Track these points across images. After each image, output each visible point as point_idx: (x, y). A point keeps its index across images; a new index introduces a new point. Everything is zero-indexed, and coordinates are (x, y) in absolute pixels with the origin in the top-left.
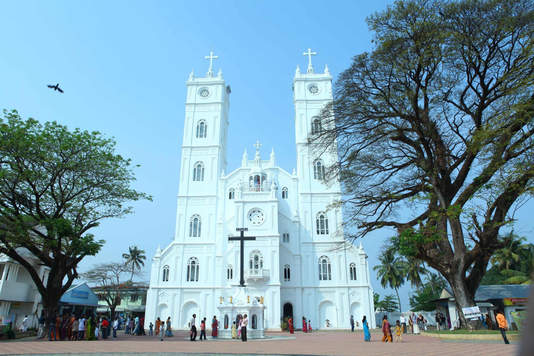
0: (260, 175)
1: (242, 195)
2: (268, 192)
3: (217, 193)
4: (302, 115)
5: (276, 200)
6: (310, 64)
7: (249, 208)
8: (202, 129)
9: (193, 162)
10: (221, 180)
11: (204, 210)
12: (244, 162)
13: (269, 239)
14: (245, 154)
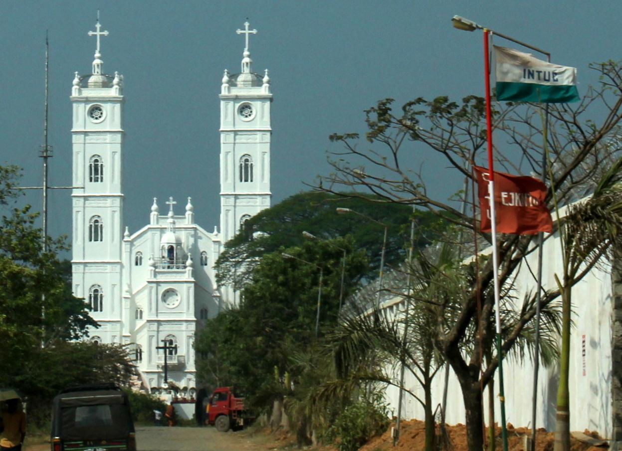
0: (174, 246)
1: (156, 274)
2: (183, 270)
3: (121, 258)
4: (227, 153)
5: (193, 280)
6: (246, 49)
7: (163, 288)
8: (96, 171)
9: (88, 218)
10: (125, 241)
11: (106, 280)
12: (154, 215)
13: (185, 324)
14: (154, 207)
